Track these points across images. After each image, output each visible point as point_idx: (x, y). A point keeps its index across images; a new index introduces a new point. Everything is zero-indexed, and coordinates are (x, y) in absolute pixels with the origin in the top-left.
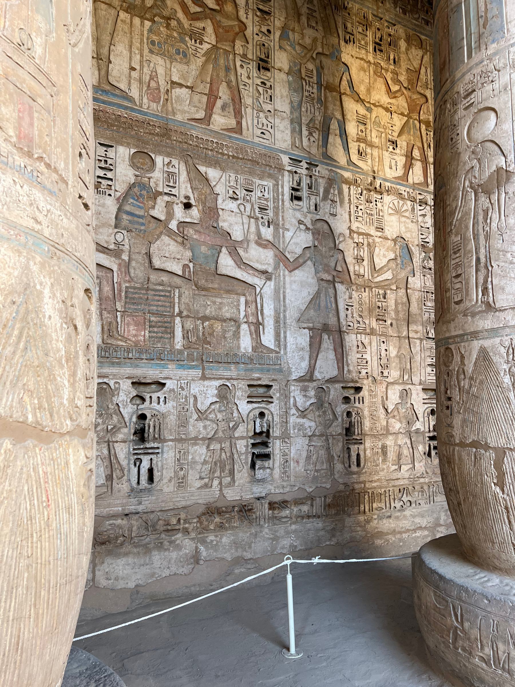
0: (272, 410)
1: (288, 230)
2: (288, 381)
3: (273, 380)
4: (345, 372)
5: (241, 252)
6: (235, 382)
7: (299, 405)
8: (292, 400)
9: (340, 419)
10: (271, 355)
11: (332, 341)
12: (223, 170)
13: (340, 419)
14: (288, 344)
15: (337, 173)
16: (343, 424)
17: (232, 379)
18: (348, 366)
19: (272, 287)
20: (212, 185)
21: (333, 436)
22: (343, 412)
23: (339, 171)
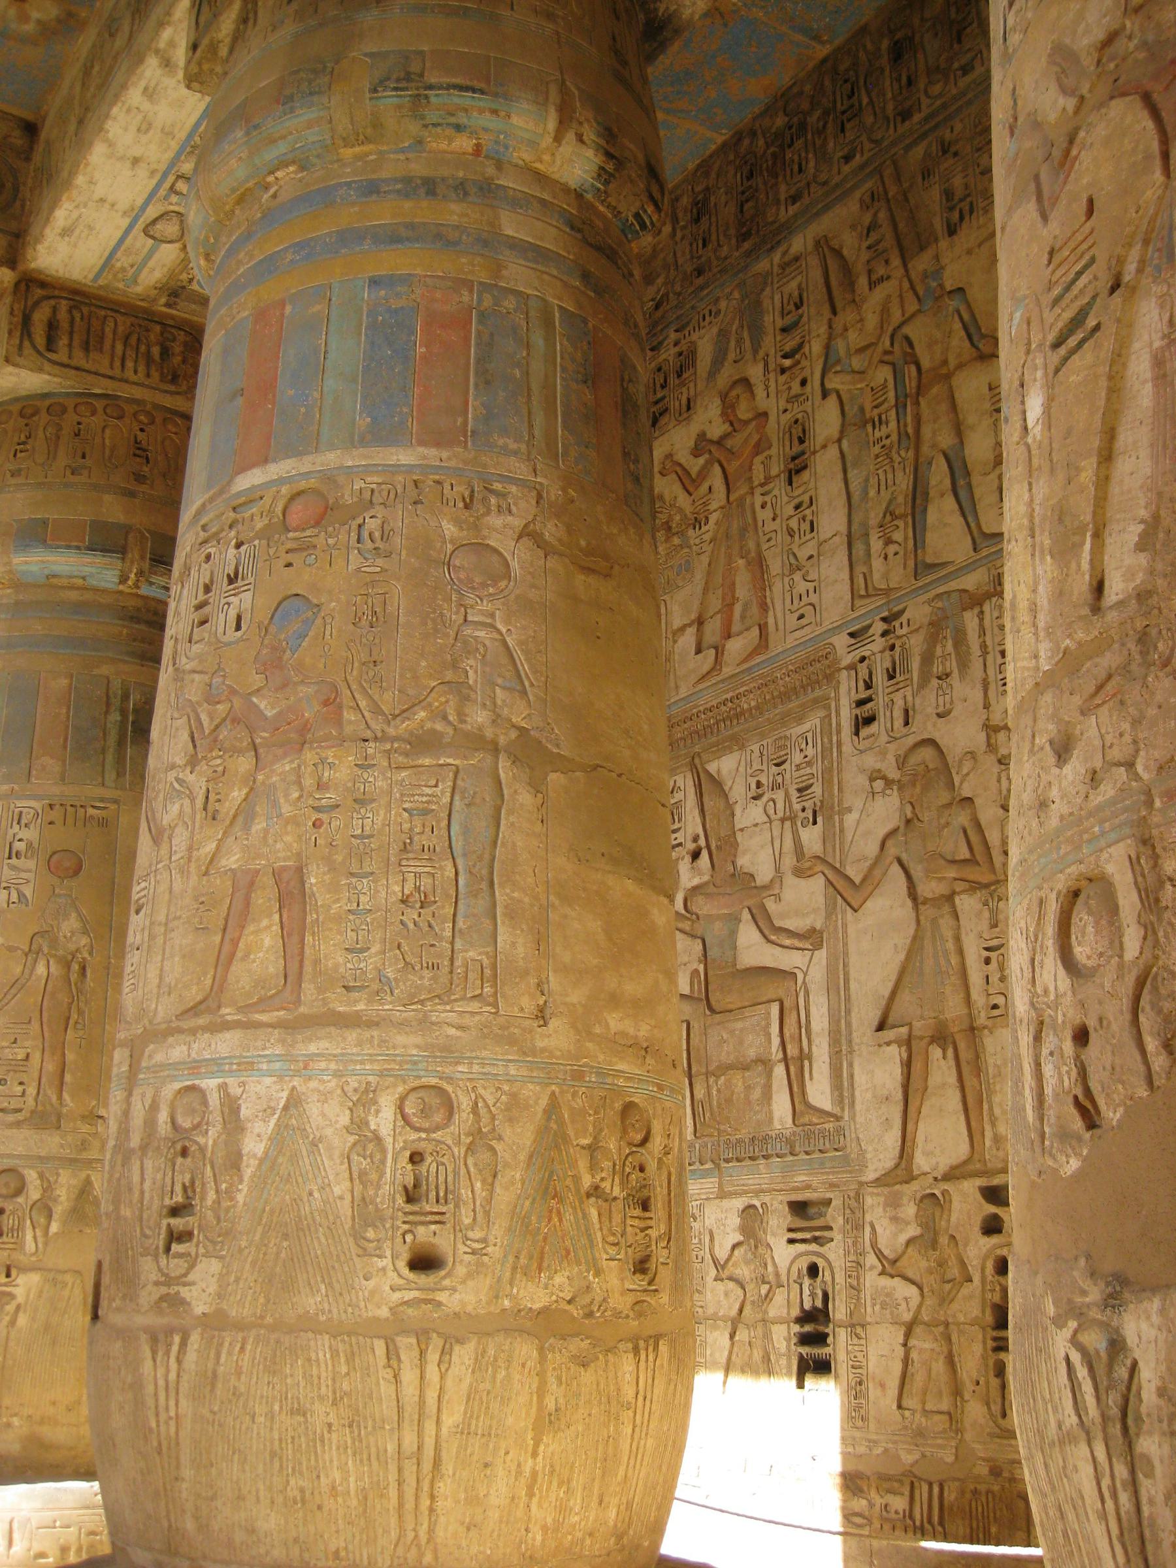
0: (832, 1257)
1: (849, 810)
2: (861, 1184)
3: (833, 1186)
4: (988, 1143)
5: (771, 905)
6: (767, 1199)
7: (882, 1244)
8: (868, 1229)
9: (977, 1279)
10: (826, 1126)
11: (952, 1063)
12: (742, 747)
13: (977, 1279)
14: (857, 1093)
15: (948, 593)
16: (983, 1291)
17: (763, 1191)
18: (993, 1125)
19: (824, 962)
20: (726, 788)
21: (958, 1324)
22: (985, 1259)
23: (954, 585)
